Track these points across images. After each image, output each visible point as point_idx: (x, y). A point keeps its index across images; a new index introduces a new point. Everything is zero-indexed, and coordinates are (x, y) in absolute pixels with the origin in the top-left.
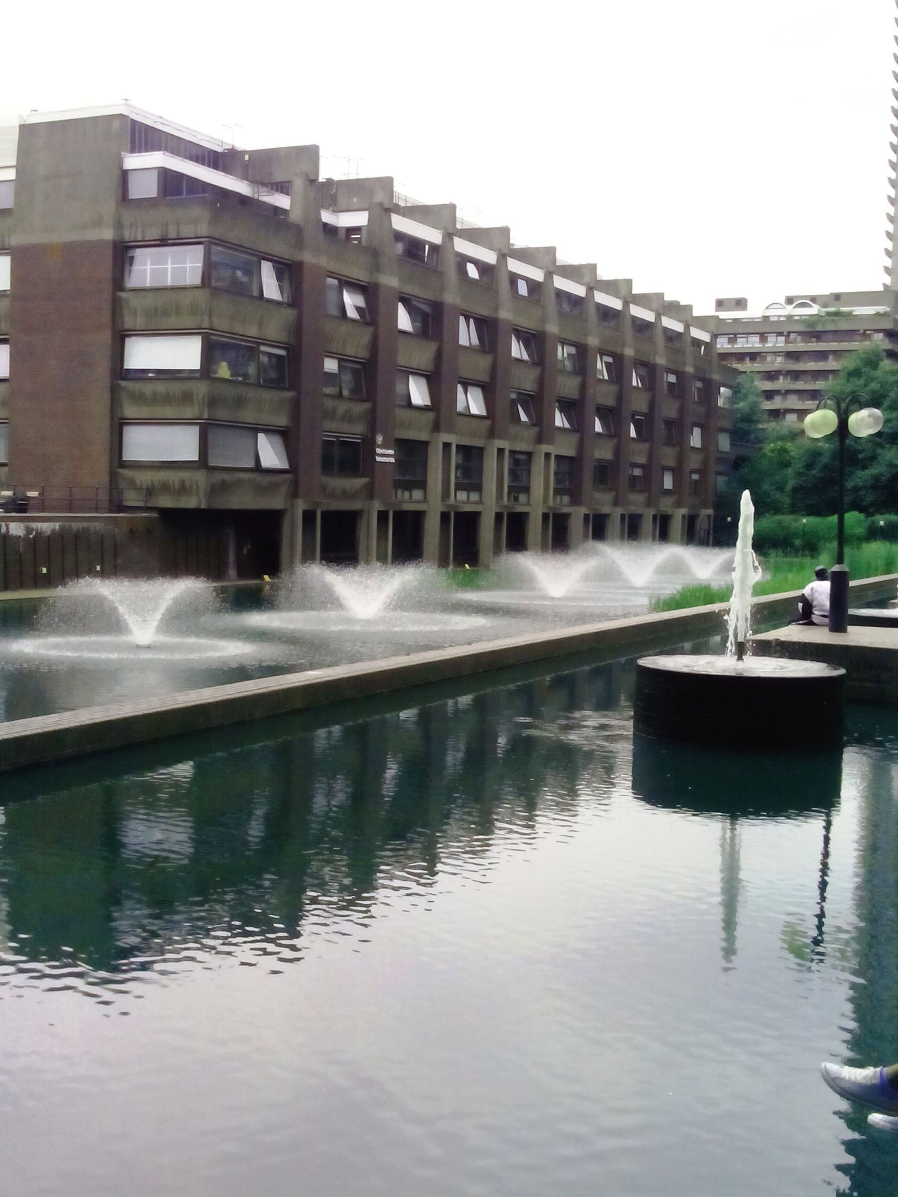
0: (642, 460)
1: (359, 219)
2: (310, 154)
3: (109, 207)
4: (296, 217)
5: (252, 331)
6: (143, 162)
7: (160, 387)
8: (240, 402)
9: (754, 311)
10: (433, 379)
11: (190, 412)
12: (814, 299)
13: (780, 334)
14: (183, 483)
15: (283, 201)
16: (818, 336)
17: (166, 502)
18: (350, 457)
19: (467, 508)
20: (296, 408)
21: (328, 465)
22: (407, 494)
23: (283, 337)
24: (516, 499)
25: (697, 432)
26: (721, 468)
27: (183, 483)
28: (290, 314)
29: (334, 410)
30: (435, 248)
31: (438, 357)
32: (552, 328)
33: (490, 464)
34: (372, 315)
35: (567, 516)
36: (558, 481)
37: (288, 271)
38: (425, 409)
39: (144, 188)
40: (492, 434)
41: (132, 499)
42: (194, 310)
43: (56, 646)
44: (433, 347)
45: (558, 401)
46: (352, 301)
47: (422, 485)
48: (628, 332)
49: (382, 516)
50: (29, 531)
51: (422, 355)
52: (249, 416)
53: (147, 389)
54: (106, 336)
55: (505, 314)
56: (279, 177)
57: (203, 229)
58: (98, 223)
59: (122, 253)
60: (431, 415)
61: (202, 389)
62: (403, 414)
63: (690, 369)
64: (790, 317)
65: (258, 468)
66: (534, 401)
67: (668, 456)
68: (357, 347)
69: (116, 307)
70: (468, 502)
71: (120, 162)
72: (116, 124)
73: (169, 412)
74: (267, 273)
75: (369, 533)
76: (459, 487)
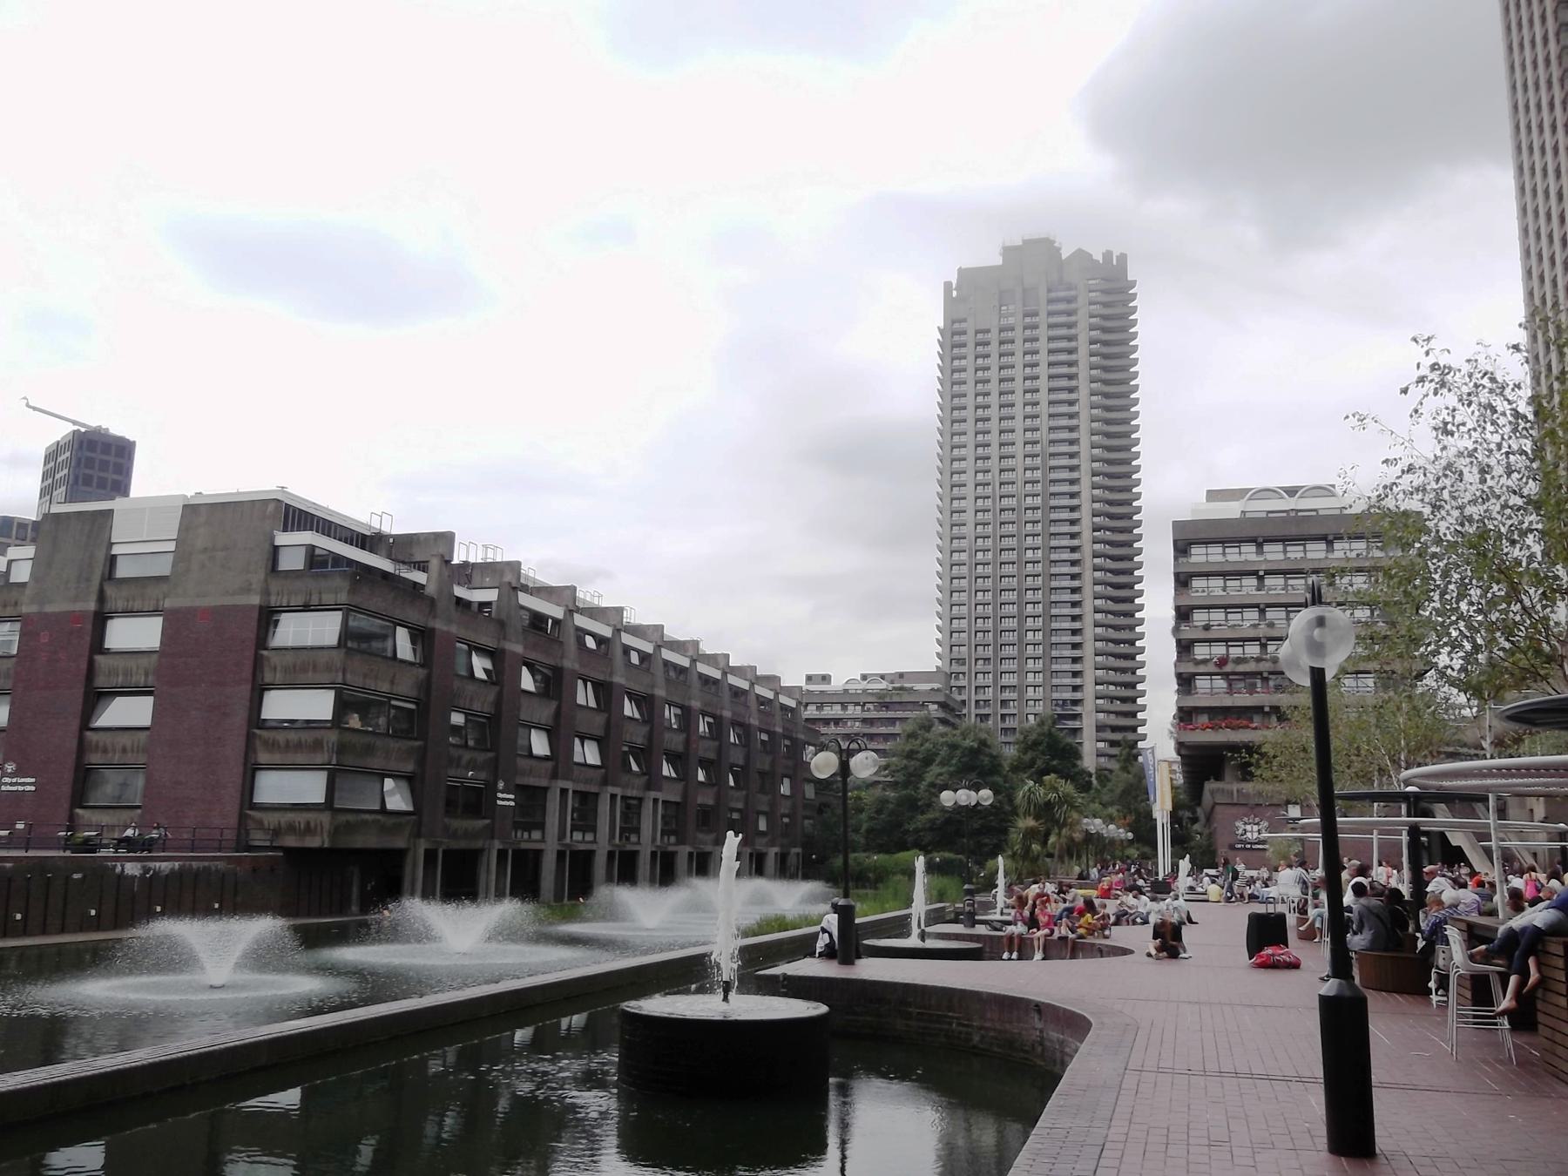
0: (740, 805)
1: (491, 595)
2: (447, 539)
3: (258, 577)
4: (431, 590)
5: (385, 687)
6: (294, 542)
7: (293, 736)
8: (369, 750)
9: (837, 683)
10: (552, 733)
11: (320, 758)
12: (883, 677)
13: (857, 704)
14: (308, 823)
15: (419, 577)
16: (886, 706)
17: (291, 841)
18: (477, 802)
19: (582, 847)
20: (422, 757)
21: (451, 807)
22: (526, 835)
23: (414, 693)
24: (628, 839)
25: (786, 781)
26: (808, 813)
27: (308, 823)
28: (422, 672)
29: (460, 758)
30: (556, 622)
31: (558, 714)
32: (660, 692)
33: (604, 807)
34: (495, 677)
36: (665, 823)
37: (420, 636)
38: (546, 758)
39: (292, 561)
40: (605, 782)
41: (258, 838)
42: (329, 668)
43: (137, 988)
44: (554, 704)
46: (480, 665)
47: (541, 826)
48: (726, 696)
49: (502, 854)
50: (146, 870)
51: (544, 712)
52: (376, 763)
53: (281, 737)
54: (245, 690)
55: (618, 679)
56: (418, 558)
57: (343, 598)
58: (247, 590)
59: (267, 618)
60: (550, 764)
61: (332, 737)
62: (523, 763)
63: (779, 730)
64: (864, 691)
65: (383, 810)
66: (646, 754)
67: (763, 802)
68: (484, 702)
69: (258, 664)
70: (583, 841)
71: (272, 538)
72: (271, 507)
73: (300, 758)
74: (402, 635)
75: (489, 871)
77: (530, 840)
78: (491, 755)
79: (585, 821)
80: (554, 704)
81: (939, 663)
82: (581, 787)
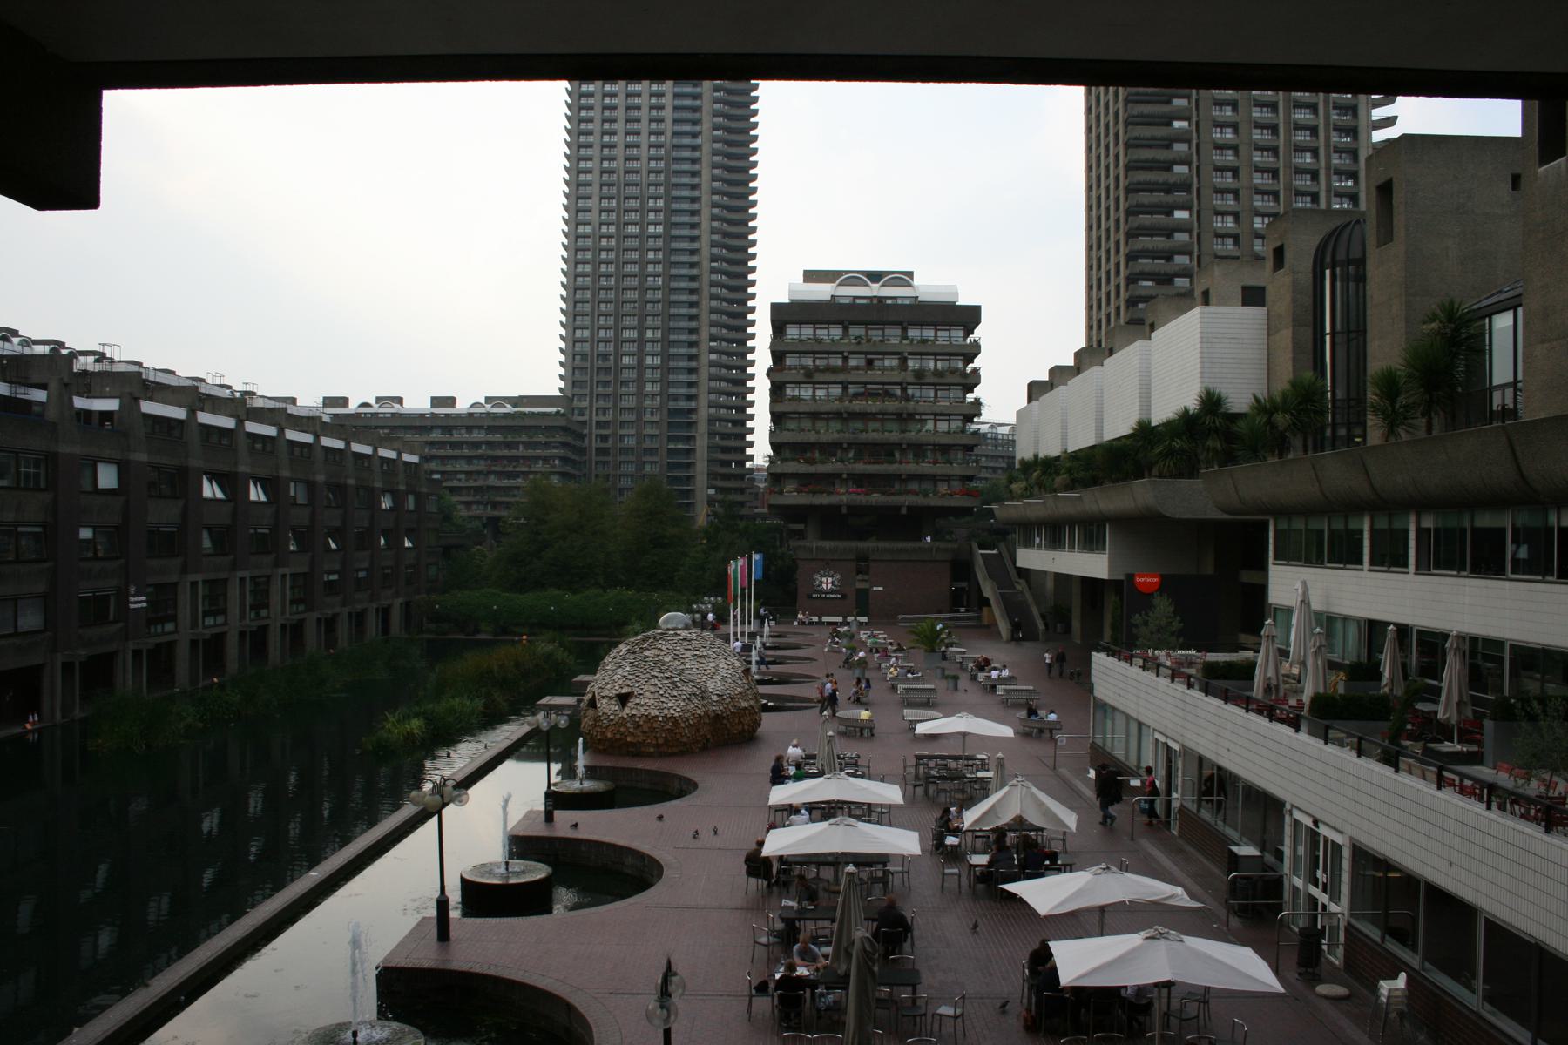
0: (366, 565)
1: (111, 405)
9: (463, 406)
15: (40, 396)
32: (285, 473)
33: (234, 592)
35: (301, 623)
44: (181, 503)
45: (293, 530)
47: (174, 618)
55: (242, 469)
63: (402, 487)
76: (205, 614)
77: (164, 633)
78: (122, 561)
79: (216, 605)
80: (181, 503)
81: (562, 385)
82: (212, 576)
